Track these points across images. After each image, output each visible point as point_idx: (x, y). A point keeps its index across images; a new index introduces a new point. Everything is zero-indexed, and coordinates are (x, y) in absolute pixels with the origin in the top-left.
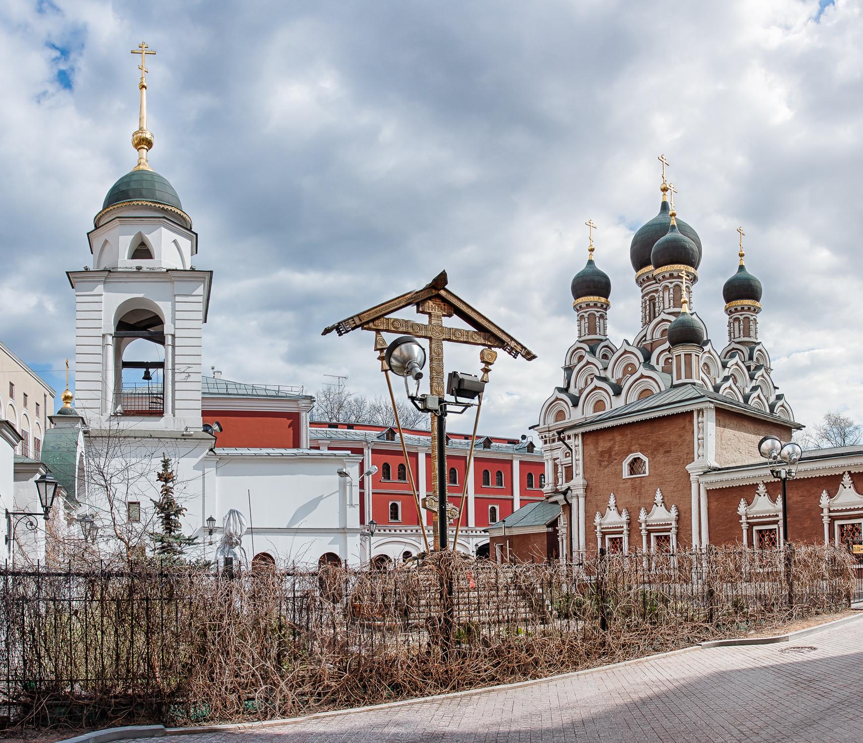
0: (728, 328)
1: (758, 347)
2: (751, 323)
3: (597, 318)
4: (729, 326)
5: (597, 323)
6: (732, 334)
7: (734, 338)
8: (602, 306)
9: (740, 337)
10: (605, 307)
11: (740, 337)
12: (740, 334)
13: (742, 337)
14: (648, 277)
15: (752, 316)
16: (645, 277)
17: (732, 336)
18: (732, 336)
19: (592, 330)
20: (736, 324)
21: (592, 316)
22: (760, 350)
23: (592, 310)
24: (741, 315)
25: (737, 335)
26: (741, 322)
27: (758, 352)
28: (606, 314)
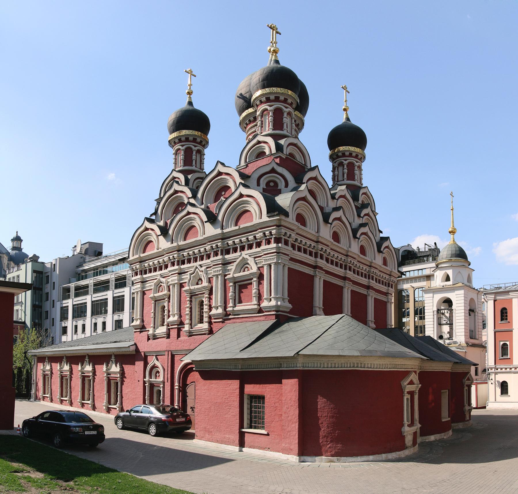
0: (331, 174)
1: (362, 191)
2: (356, 168)
3: (194, 153)
4: (333, 171)
5: (194, 157)
6: (336, 177)
7: (337, 182)
8: (201, 142)
9: (343, 180)
10: (203, 143)
11: (343, 180)
12: (343, 176)
13: (345, 180)
14: (250, 121)
15: (357, 162)
16: (247, 122)
17: (336, 180)
18: (336, 180)
19: (187, 161)
20: (341, 169)
21: (188, 153)
22: (364, 194)
23: (191, 145)
24: (346, 160)
25: (340, 178)
26: (345, 167)
27: (364, 195)
28: (204, 151)
